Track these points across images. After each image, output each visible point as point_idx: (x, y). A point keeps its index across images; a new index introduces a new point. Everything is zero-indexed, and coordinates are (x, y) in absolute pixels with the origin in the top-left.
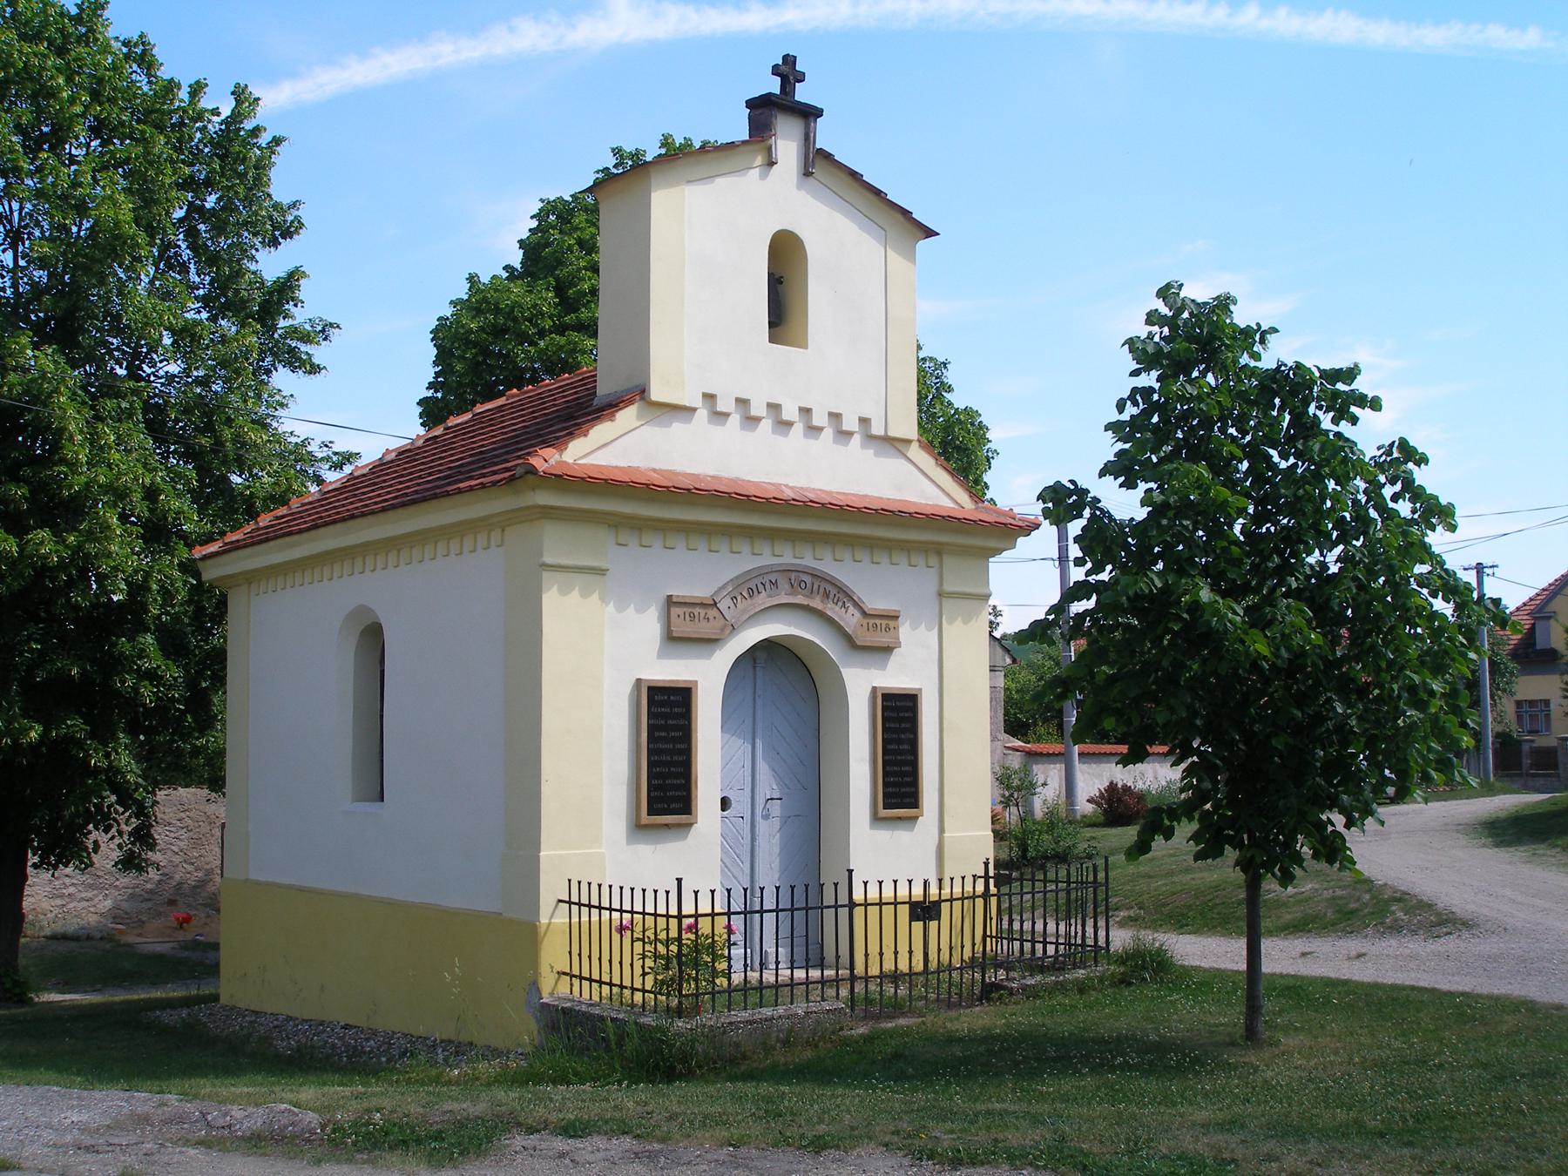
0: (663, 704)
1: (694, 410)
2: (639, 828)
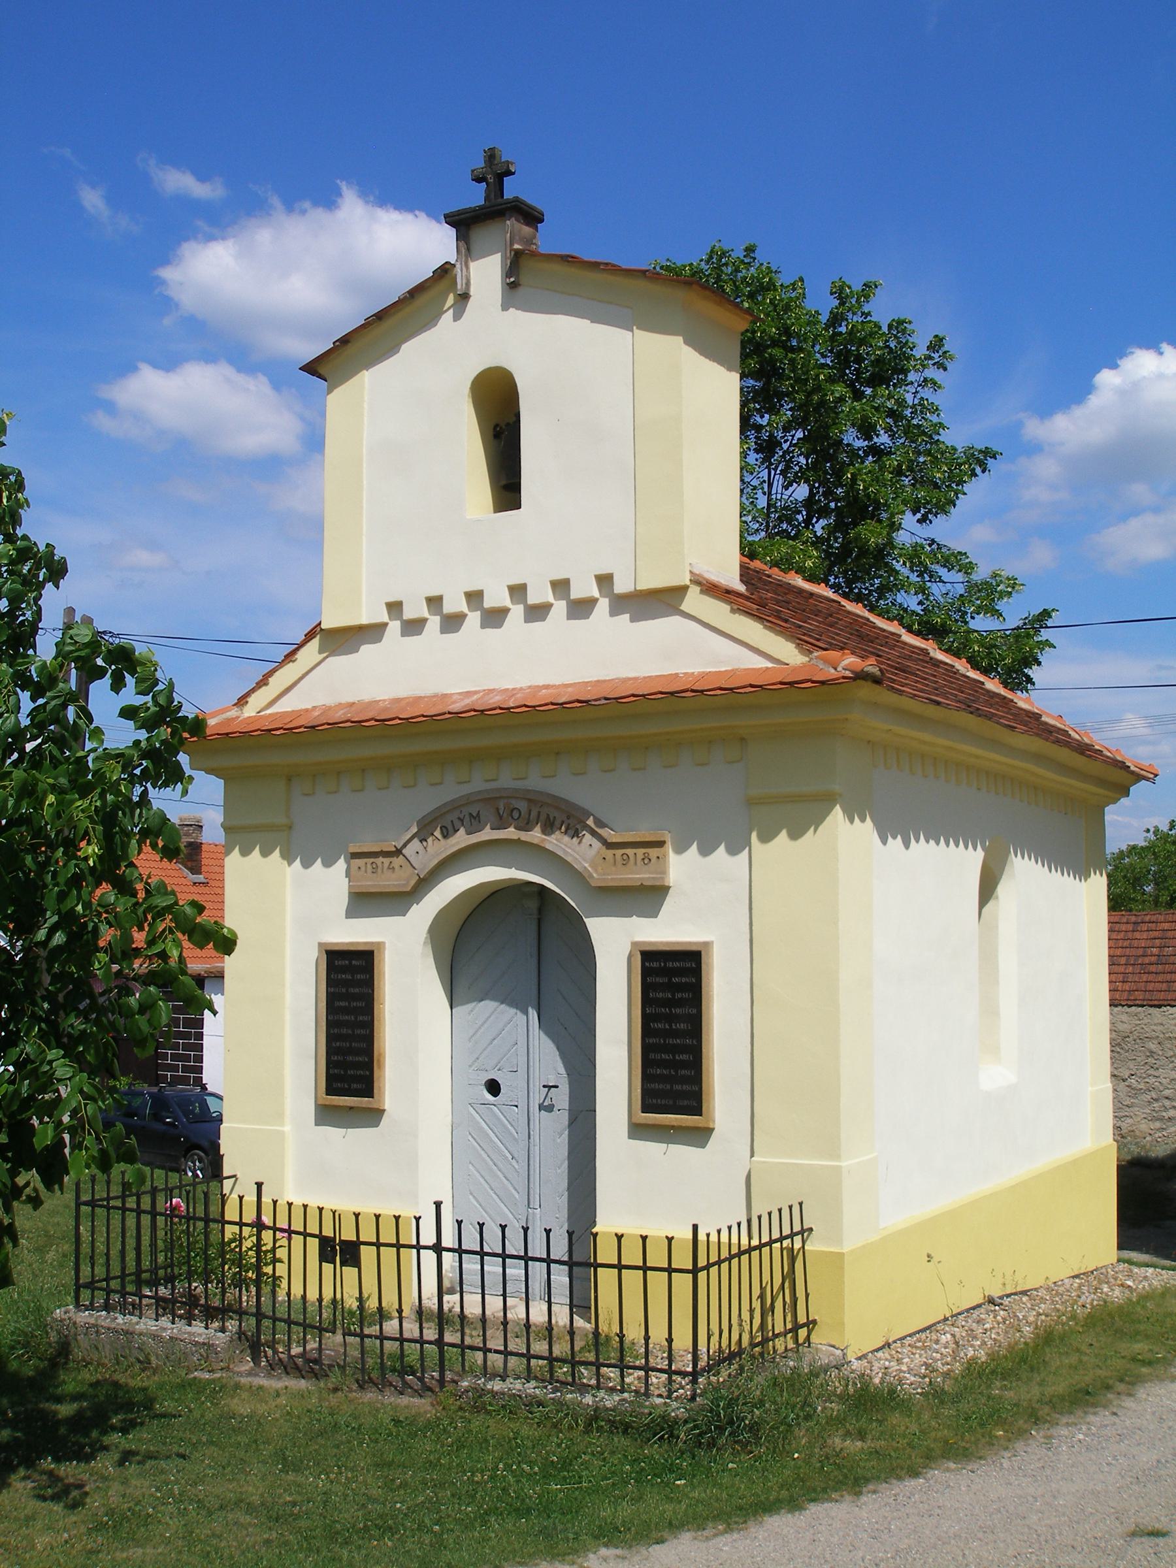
0: (343, 970)
1: (385, 625)
2: (326, 1115)
